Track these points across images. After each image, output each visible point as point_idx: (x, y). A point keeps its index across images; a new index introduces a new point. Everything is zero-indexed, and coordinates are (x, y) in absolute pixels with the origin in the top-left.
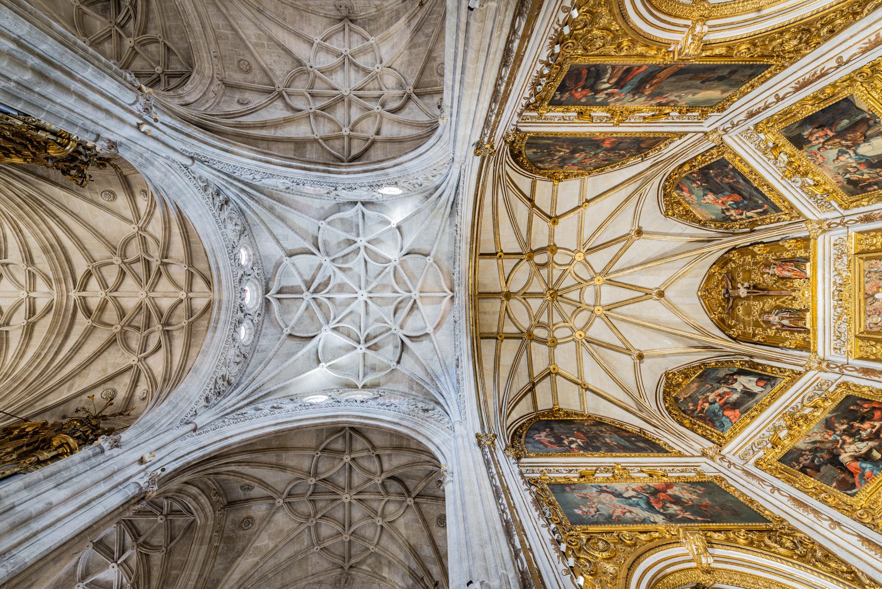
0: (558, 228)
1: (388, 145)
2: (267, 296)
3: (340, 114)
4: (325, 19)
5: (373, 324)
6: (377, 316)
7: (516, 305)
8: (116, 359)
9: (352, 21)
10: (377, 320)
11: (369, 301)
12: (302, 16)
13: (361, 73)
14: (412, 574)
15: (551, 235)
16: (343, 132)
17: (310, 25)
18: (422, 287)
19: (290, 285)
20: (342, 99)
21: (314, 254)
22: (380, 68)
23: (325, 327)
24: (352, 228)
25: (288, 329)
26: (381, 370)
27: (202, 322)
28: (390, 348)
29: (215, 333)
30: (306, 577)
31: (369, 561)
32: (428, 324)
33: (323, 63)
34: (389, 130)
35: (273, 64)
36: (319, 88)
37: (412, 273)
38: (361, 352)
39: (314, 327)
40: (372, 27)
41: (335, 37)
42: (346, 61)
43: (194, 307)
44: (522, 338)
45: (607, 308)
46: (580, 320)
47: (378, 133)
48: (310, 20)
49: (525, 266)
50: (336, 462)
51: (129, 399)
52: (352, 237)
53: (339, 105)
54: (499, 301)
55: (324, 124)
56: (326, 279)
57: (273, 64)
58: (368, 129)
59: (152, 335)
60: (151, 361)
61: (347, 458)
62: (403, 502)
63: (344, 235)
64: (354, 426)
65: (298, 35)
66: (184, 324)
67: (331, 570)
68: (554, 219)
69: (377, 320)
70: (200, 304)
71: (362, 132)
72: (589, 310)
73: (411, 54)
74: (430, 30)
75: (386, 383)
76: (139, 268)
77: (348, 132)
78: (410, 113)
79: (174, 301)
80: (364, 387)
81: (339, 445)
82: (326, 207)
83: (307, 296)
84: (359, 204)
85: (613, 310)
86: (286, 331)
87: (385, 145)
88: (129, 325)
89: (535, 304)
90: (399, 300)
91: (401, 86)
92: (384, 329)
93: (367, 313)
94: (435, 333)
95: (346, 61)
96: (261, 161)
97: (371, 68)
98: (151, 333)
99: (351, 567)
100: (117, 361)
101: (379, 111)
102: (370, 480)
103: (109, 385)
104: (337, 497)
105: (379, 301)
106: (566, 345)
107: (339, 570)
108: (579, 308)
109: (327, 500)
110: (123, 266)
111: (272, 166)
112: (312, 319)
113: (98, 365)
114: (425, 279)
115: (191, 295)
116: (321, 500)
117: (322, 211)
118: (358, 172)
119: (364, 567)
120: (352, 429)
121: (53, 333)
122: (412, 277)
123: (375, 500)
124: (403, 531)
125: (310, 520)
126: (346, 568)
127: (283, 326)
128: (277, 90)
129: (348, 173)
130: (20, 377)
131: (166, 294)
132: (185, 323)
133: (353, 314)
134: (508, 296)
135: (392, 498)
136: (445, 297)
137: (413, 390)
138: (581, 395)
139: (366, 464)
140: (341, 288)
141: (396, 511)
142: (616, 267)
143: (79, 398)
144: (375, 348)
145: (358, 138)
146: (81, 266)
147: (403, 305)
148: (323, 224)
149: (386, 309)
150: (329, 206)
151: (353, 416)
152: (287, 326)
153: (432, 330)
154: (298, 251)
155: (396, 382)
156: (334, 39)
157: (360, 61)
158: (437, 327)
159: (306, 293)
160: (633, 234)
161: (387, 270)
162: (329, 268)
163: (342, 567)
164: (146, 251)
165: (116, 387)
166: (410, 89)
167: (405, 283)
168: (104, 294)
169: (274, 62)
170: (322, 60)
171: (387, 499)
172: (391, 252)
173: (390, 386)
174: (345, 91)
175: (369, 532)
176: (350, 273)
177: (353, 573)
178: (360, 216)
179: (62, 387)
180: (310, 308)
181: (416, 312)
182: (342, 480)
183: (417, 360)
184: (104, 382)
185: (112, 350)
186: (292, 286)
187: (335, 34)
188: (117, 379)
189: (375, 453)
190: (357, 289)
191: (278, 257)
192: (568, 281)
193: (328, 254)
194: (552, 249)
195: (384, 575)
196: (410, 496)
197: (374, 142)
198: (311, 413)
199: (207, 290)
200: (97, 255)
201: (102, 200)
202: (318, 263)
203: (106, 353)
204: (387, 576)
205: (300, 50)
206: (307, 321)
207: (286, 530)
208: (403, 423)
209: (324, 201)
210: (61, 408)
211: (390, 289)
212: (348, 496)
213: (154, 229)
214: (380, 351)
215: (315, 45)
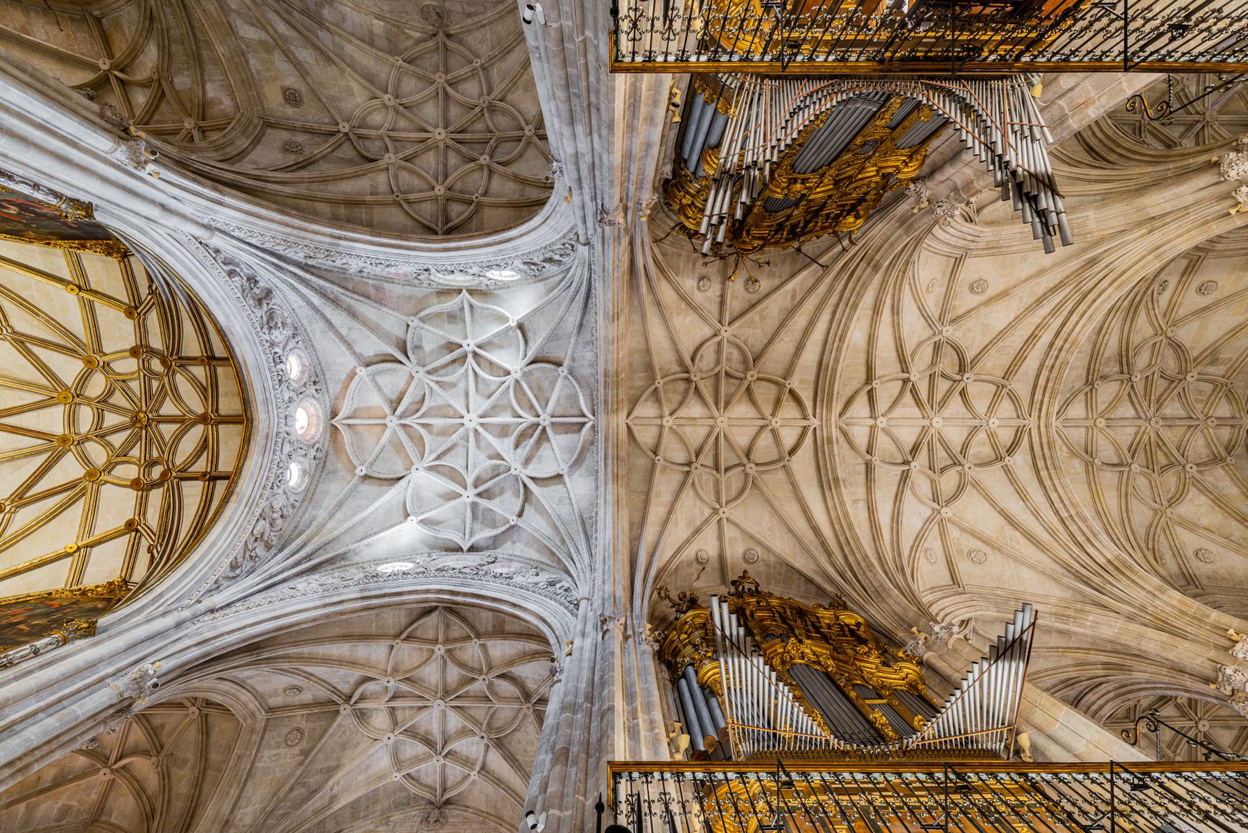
0: (129, 515)
1: (373, 630)
2: (333, 422)
3: (454, 673)
4: (469, 804)
5: (459, 380)
6: (453, 391)
7: (196, 405)
8: (752, 332)
9: (432, 803)
10: (453, 385)
11: (464, 412)
12: (495, 808)
13: (422, 731)
14: (321, 24)
15: (142, 506)
16: (443, 649)
17: (487, 796)
18: (384, 431)
19: (569, 435)
20: (446, 693)
21: (532, 478)
22: (386, 737)
23: (518, 375)
24: (483, 514)
25: (562, 375)
26: (438, 315)
27: (642, 383)
28: (428, 347)
29: (606, 369)
30: (491, 23)
31: (410, 43)
32: (367, 380)
33: (472, 744)
34: (376, 652)
35: (535, 740)
36: (479, 711)
37: (398, 452)
38: (469, 341)
39: (536, 376)
40: (404, 794)
41: (458, 780)
42: (439, 747)
43: (656, 405)
44: (181, 358)
45: (52, 402)
46: (97, 384)
47: (392, 647)
48: (486, 802)
49: (179, 460)
50: (458, 186)
51: (726, 279)
52: (483, 503)
53: (453, 686)
54: (223, 411)
55: (473, 660)
56: (523, 444)
57: (535, 740)
58: (407, 653)
59: (712, 365)
60: (707, 332)
61: (440, 190)
62: (360, 127)
63: (492, 505)
64: (435, 237)
65: (498, 781)
66: (661, 382)
67: (463, 32)
68: (130, 526)
69: (453, 385)
70: (646, 410)
71: (421, 649)
72: (87, 398)
73: (339, 759)
74: (296, 792)
75: (426, 297)
76: (726, 457)
77: (436, 648)
78: (346, 676)
79: (681, 413)
80: (459, 291)
81: (455, 208)
82: (509, 543)
83: (545, 420)
84: (465, 548)
85: (46, 398)
86: (563, 371)
87: (379, 632)
88: (741, 379)
89: (169, 408)
90: (419, 414)
91: (362, 716)
92: (441, 372)
93: (467, 394)
94: (355, 367)
95: (439, 747)
96: (520, 607)
97: (401, 737)
98: (713, 369)
99: (435, 35)
100: (752, 330)
101: (387, 679)
102: (406, 159)
103: (755, 298)
104: (454, 136)
105: (451, 413)
106: (120, 347)
107: (452, 32)
108: (103, 402)
109: (473, 132)
110: (745, 460)
111: (513, 600)
112: (539, 388)
113: (771, 325)
114: (377, 443)
115: (658, 421)
116: (481, 132)
117: (515, 538)
118: (410, 593)
119: (417, 35)
120: (436, 233)
121: (832, 369)
122: (398, 447)
123: (403, 130)
124: (353, 85)
125: (487, 104)
126: (441, 34)
127: (570, 377)
128: (530, 705)
129: (427, 591)
130: (851, 308)
131: (691, 422)
132: (660, 382)
133: (487, 393)
134: (204, 419)
135: (373, 132)
136: (349, 418)
137: (373, 286)
138: (83, 274)
139: (416, 182)
140: (503, 431)
141: (370, 113)
142: (40, 460)
143: (783, 279)
144: (451, 346)
145: (425, 641)
146: (803, 464)
147: (415, 407)
148: (513, 520)
149: (440, 402)
150: (505, 546)
151: (422, 250)
152: (566, 377)
153: (358, 370)
154: (552, 482)
155: (410, 298)
156: (459, 777)
157: (421, 748)
158: (352, 375)
159: (546, 423)
160: (8, 508)
161: (434, 456)
162: (514, 459)
163: (449, 36)
164: (717, 483)
165: (747, 296)
166: (345, 710)
167: (411, 438)
168: (773, 422)
169: (533, 744)
170: (475, 748)
171: (381, 131)
172: (423, 480)
173: (419, 292)
174: (438, 706)
175: (409, 84)
176: (491, 452)
177: (430, 28)
178: (467, 532)
180: (543, 403)
181: (394, 397)
182: (453, 160)
183: (374, 329)
184: (759, 301)
185: (758, 347)
186: (566, 433)
187: (458, 783)
188: (747, 305)
189: (394, 196)
190: (480, 429)
191: (577, 474)
192: (117, 440)
193: (516, 478)
194: (136, 484)
195: (382, 23)
196: (346, 134)
197: (397, 636)
198: (479, 255)
199: (635, 429)
200: (781, 475)
201: (759, 550)
202: (530, 467)
203: (765, 341)
204: (375, 21)
205: (496, 761)
206: (545, 385)
207: (521, 92)
208: (328, 240)
209: (510, 552)
210: (798, 267)
211: (435, 429)
212: (439, 137)
213: (702, 512)
214: (444, 342)
215: (478, 768)
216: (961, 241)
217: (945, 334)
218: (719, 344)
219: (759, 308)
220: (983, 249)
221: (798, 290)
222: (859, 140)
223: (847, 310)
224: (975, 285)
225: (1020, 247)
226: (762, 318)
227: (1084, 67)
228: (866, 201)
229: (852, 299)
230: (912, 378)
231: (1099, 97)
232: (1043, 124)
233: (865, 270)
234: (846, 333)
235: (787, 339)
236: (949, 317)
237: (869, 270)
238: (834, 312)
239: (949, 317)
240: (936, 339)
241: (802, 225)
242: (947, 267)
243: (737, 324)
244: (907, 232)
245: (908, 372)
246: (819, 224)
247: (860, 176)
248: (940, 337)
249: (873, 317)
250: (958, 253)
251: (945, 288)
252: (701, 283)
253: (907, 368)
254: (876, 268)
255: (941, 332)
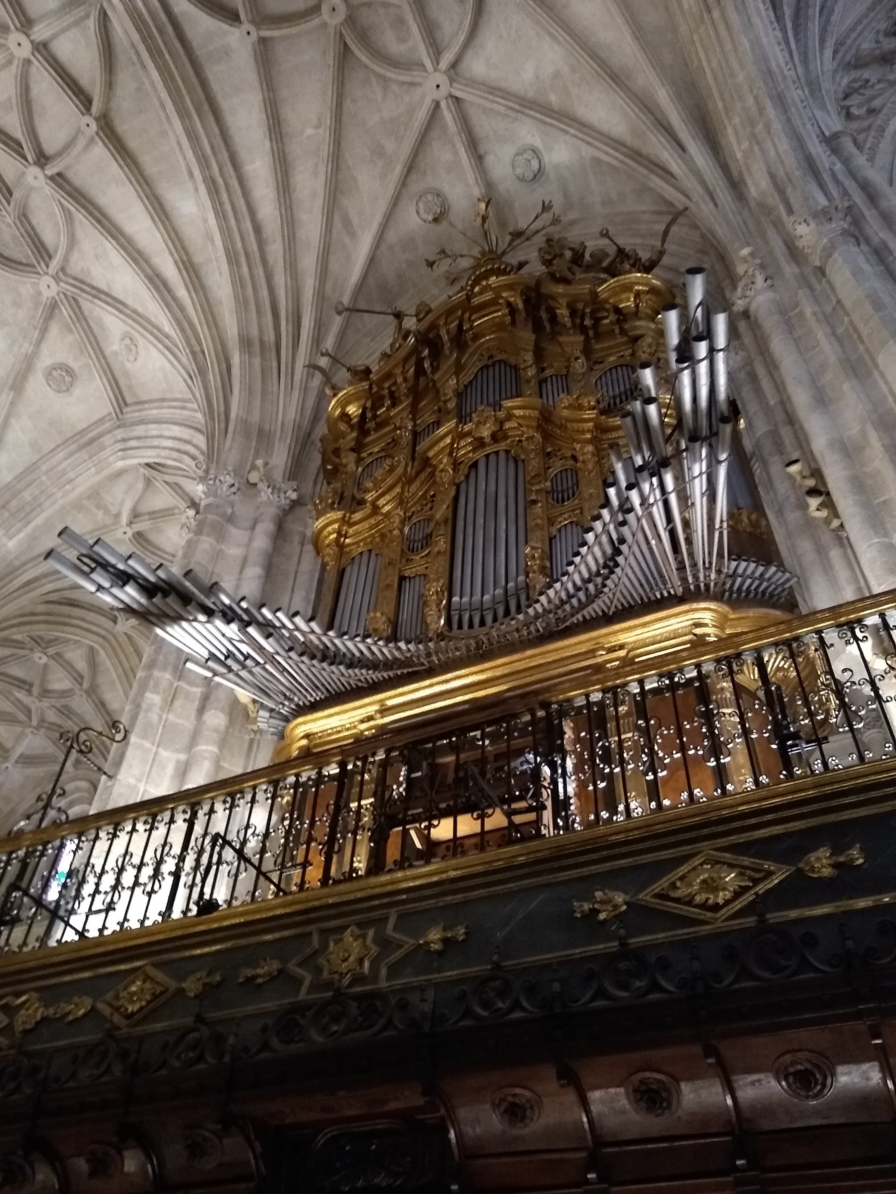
103: (416, 186)
143: (383, 247)
179: (334, 231)
184: (404, 183)
203: (348, 104)
216: (143, 434)
217: (47, 280)
218: (437, 51)
219: (398, 169)
220: (101, 435)
221: (347, 240)
222: (442, 544)
223: (239, 245)
224: (68, 379)
225: (54, 461)
226: (379, 152)
227: (243, 781)
228: (353, 450)
229: (245, 269)
230: (34, 170)
231: (161, 717)
232: (217, 679)
233: (261, 331)
234: (212, 201)
235: (309, 131)
236: (65, 311)
237: (255, 333)
238: (258, 229)
239: (65, 311)
240: (55, 264)
241: (426, 364)
242: (130, 387)
243: (422, 114)
244: (244, 423)
245: (51, 178)
246: (400, 380)
247: (398, 490)
248: (52, 269)
249: (187, 253)
250: (131, 414)
251: (108, 352)
252: (535, 164)
253: (60, 187)
254: (245, 343)
255: (56, 278)
